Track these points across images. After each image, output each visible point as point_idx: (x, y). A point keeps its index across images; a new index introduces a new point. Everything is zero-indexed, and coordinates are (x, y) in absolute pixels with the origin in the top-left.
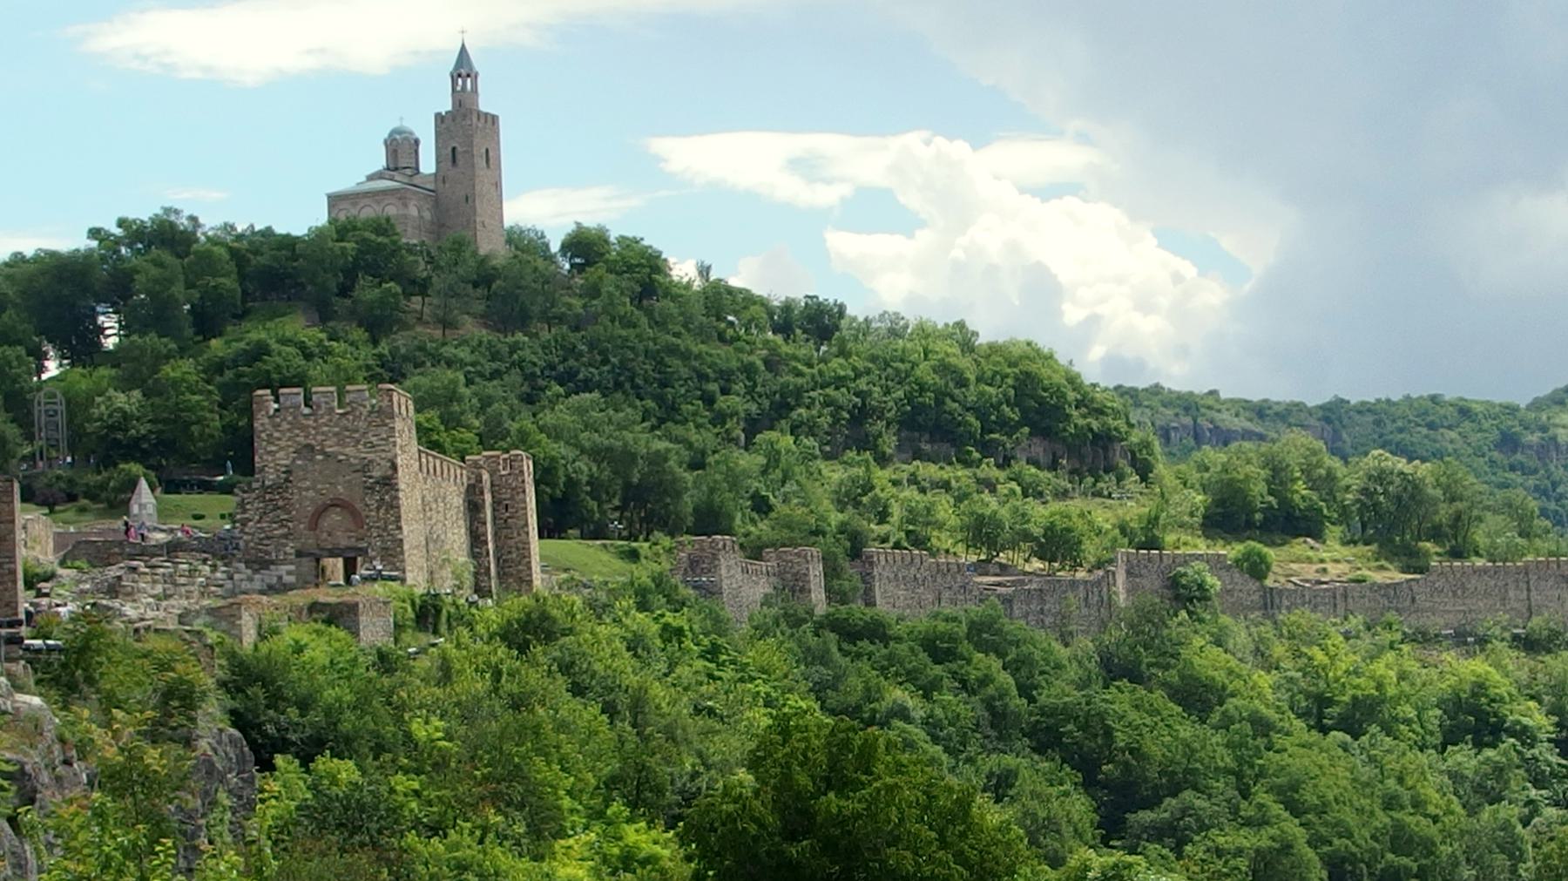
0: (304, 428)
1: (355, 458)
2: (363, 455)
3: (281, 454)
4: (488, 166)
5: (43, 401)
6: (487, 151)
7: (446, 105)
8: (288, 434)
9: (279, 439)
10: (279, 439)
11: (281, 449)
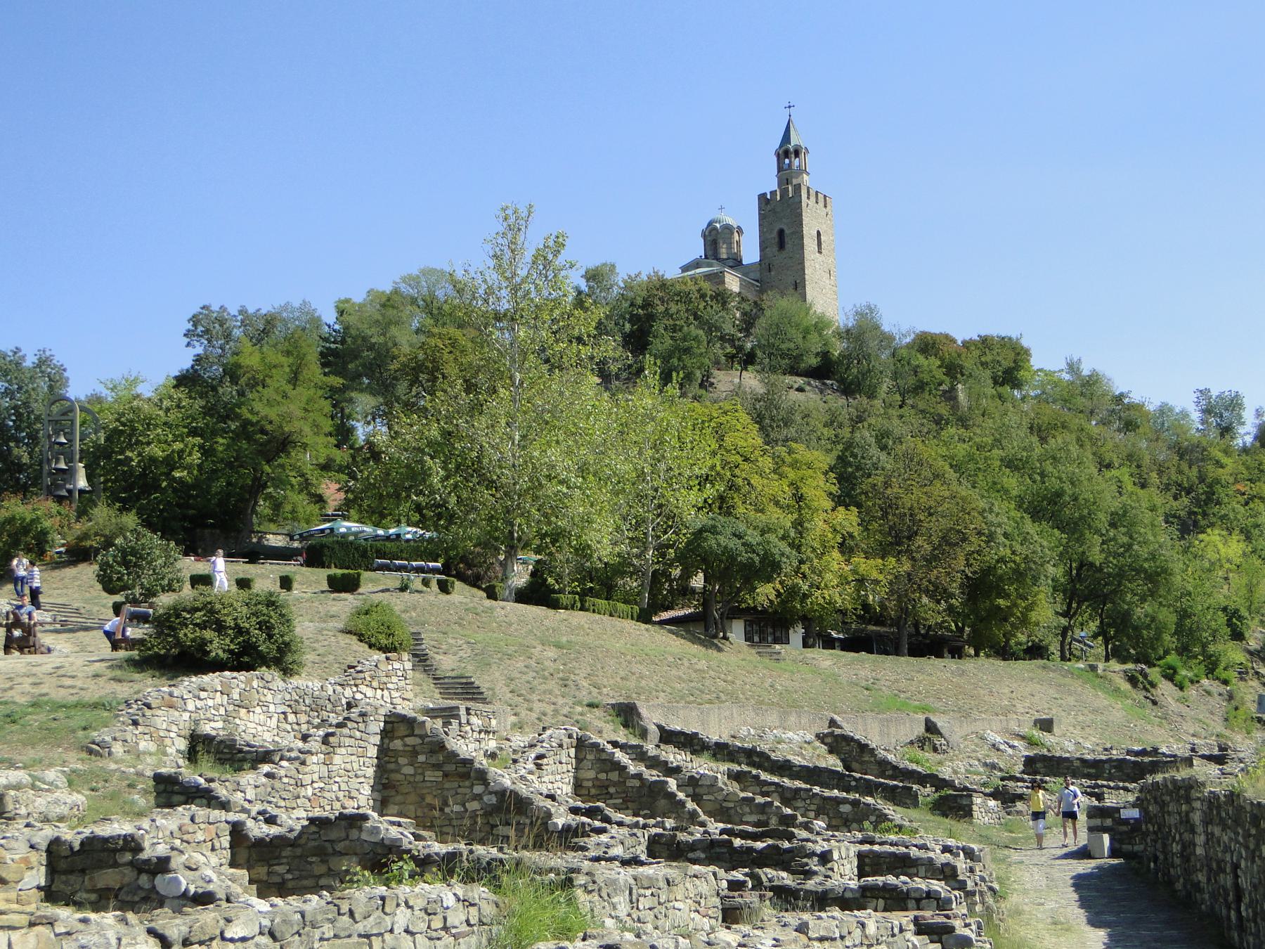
4: (820, 252)
6: (819, 233)
7: (770, 184)
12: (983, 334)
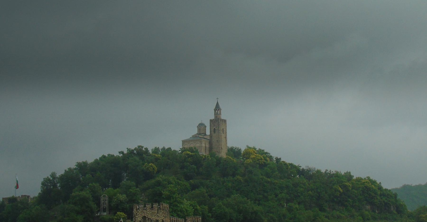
0: (144, 212)
1: (155, 219)
2: (156, 218)
3: (139, 218)
5: (103, 197)
6: (223, 129)
8: (141, 214)
9: (138, 215)
10: (138, 215)
11: (139, 217)
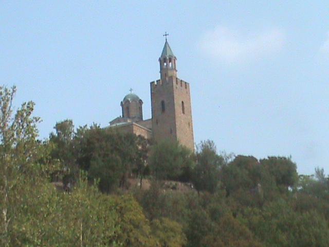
4: (183, 113)
6: (183, 102)
7: (157, 77)
12: (271, 155)
